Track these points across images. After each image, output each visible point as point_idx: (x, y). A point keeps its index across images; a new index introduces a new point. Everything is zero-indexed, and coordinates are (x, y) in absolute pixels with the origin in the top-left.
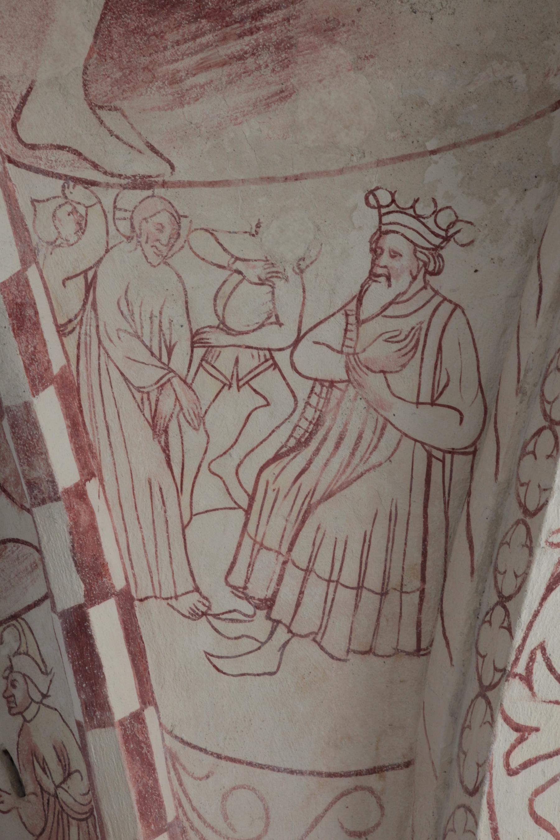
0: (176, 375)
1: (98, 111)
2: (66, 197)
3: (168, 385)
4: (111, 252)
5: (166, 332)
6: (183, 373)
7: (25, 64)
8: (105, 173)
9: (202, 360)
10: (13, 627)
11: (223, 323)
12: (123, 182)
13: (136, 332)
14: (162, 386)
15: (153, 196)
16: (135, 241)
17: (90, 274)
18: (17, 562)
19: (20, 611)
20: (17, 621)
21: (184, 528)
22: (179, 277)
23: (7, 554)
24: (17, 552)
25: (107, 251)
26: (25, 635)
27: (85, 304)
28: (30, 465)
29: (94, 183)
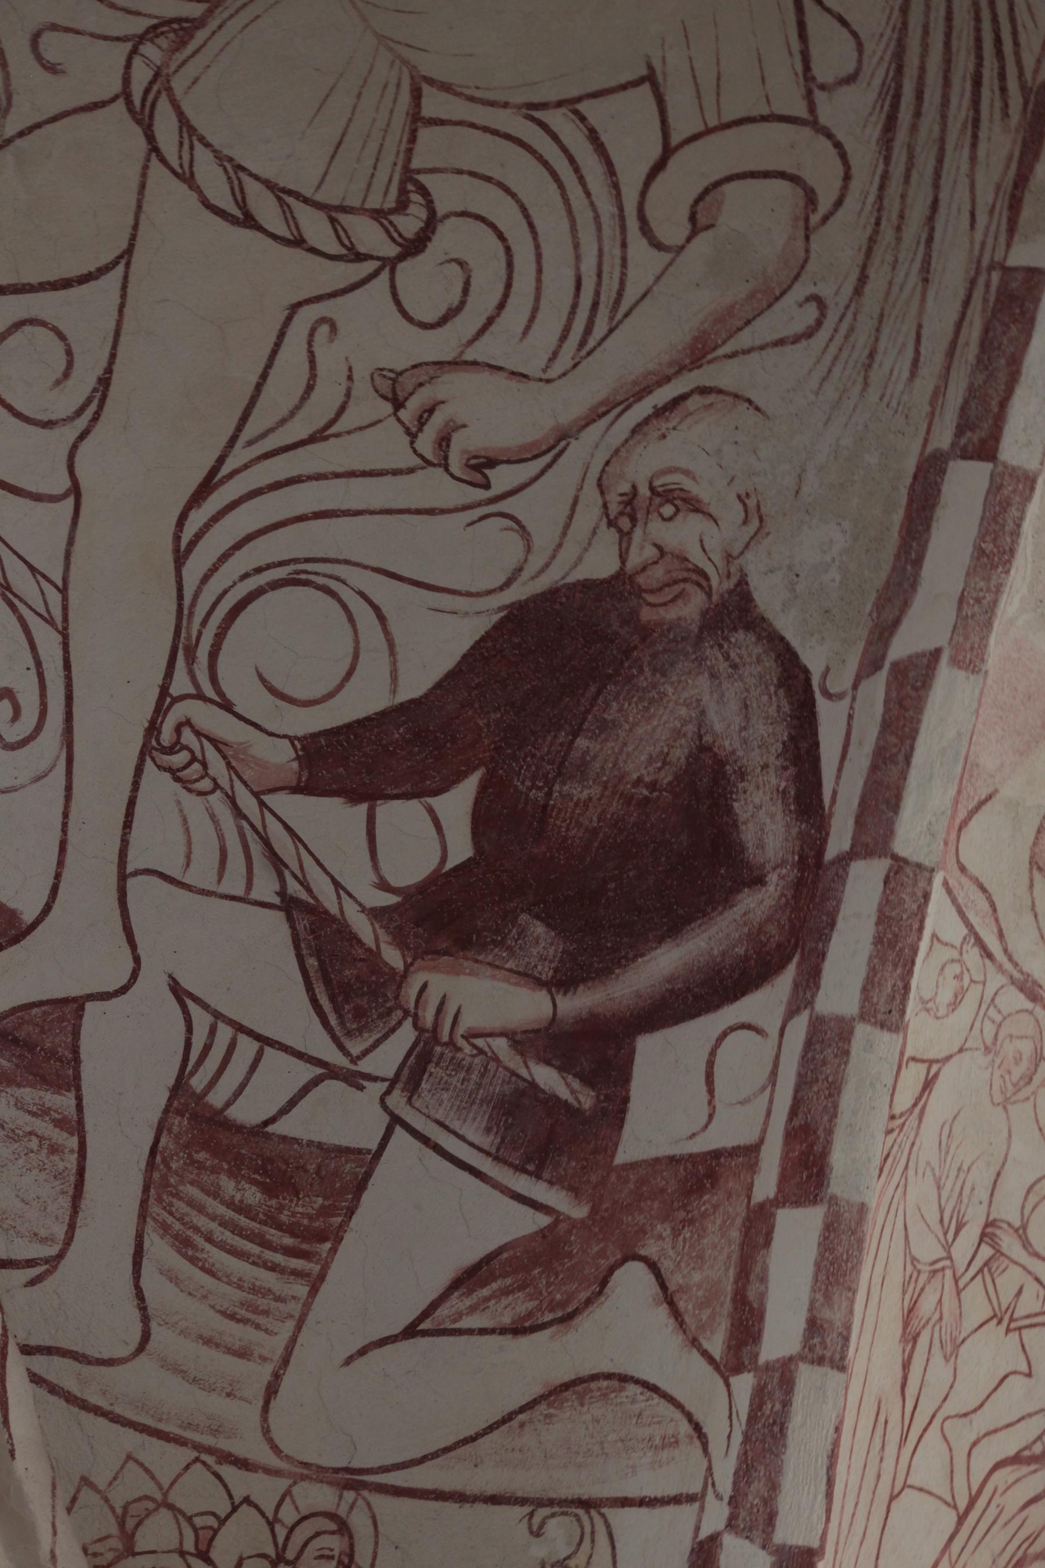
0: (953, 1267)
1: (1035, 871)
2: (961, 954)
3: (940, 1274)
4: (966, 1055)
5: (965, 1200)
6: (961, 1268)
7: (1002, 765)
8: (1006, 951)
9: (986, 1264)
10: (573, 1519)
11: (1024, 1227)
12: (1017, 975)
13: (940, 1179)
14: (935, 1272)
15: (1031, 1013)
16: (990, 1057)
17: (935, 1068)
18: (634, 1421)
19: (601, 1500)
20: (588, 1513)
21: (893, 1498)
22: (1010, 1136)
23: (619, 1400)
24: (643, 1405)
25: (961, 1051)
26: (593, 1541)
27: (915, 1105)
28: (828, 1297)
29: (989, 955)
